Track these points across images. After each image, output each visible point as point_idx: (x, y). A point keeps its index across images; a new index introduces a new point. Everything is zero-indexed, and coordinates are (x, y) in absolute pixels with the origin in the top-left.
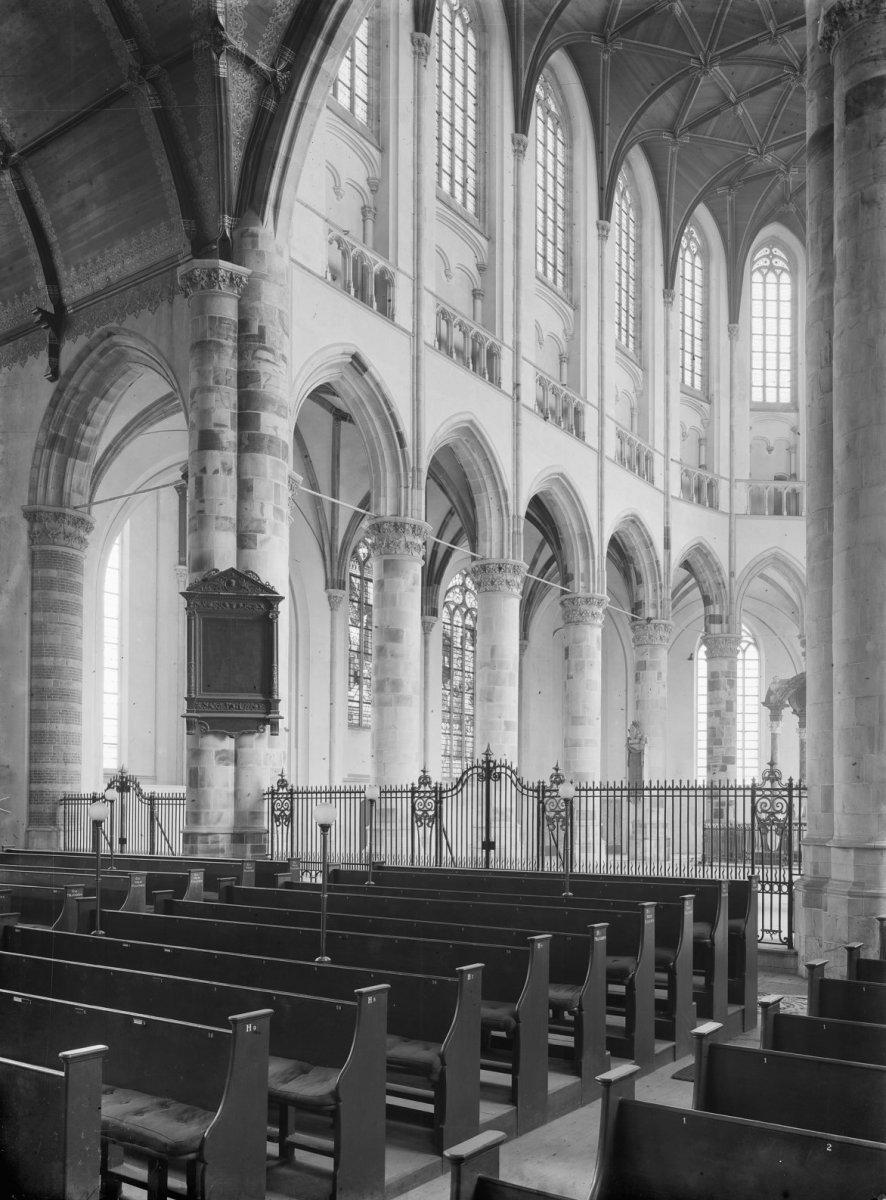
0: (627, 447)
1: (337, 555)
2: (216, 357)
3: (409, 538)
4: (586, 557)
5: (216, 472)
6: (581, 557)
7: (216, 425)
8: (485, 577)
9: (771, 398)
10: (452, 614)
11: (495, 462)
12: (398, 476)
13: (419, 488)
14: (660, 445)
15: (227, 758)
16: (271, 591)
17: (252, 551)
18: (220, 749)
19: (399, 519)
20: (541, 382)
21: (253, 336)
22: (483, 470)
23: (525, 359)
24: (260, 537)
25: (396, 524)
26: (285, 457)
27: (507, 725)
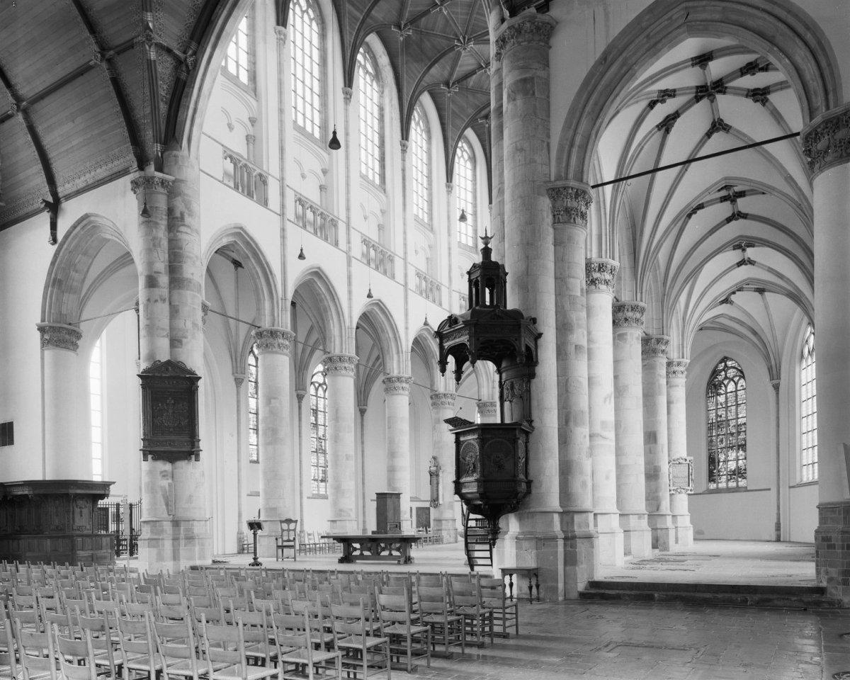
0: (424, 283)
1: (239, 355)
2: (154, 230)
3: (281, 341)
4: (398, 353)
5: (156, 301)
6: (394, 352)
7: (155, 272)
8: (333, 364)
10: (317, 389)
11: (336, 293)
12: (272, 303)
13: (286, 311)
14: (445, 281)
15: (167, 476)
16: (193, 373)
17: (180, 349)
18: (163, 470)
19: (276, 328)
20: (366, 242)
21: (177, 218)
22: (328, 297)
23: (353, 228)
24: (184, 340)
25: (271, 332)
26: (199, 291)
27: (348, 457)
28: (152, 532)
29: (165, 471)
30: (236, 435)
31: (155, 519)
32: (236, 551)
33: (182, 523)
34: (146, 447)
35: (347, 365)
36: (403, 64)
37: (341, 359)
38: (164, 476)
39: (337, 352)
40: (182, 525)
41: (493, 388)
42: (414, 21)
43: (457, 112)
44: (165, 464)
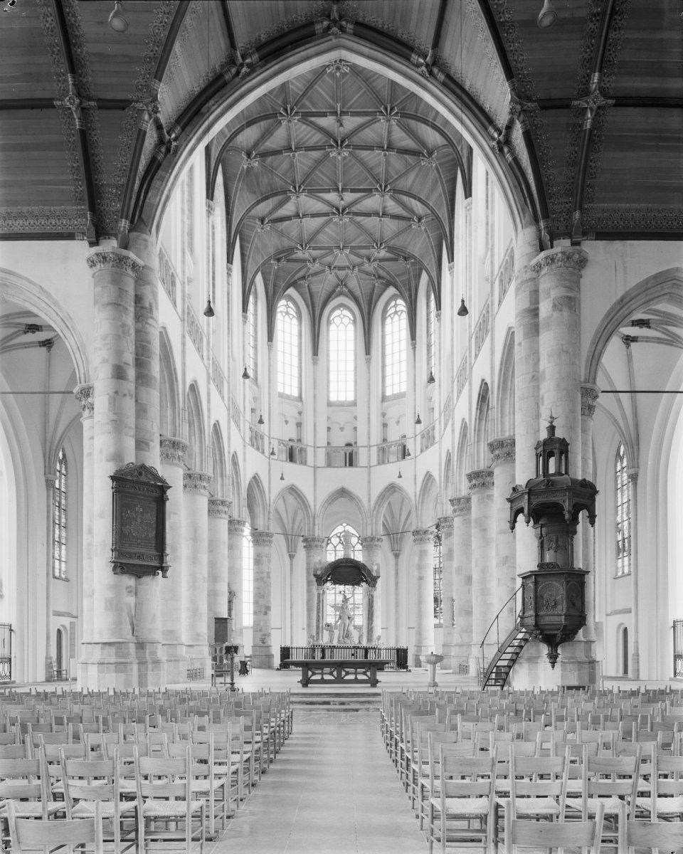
4: (222, 476)
6: (219, 476)
9: (287, 392)
18: (128, 585)
28: (117, 655)
29: (131, 586)
30: (45, 544)
31: (121, 640)
32: (44, 680)
33: (148, 646)
34: (117, 559)
35: (205, 484)
36: (236, 191)
37: (201, 477)
38: (129, 592)
39: (198, 470)
40: (147, 647)
41: (269, 519)
42: (264, 155)
43: (260, 248)
44: (130, 579)
